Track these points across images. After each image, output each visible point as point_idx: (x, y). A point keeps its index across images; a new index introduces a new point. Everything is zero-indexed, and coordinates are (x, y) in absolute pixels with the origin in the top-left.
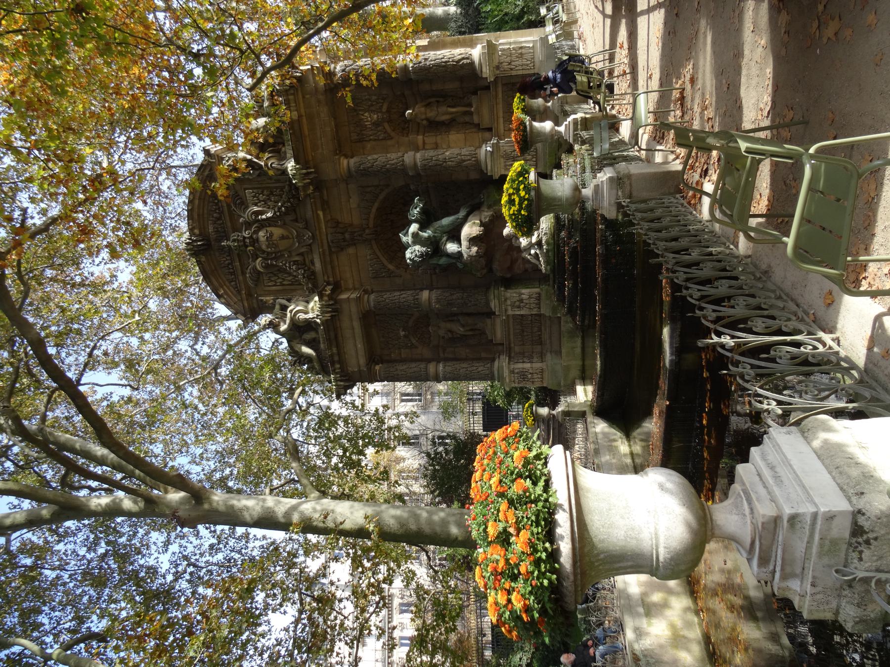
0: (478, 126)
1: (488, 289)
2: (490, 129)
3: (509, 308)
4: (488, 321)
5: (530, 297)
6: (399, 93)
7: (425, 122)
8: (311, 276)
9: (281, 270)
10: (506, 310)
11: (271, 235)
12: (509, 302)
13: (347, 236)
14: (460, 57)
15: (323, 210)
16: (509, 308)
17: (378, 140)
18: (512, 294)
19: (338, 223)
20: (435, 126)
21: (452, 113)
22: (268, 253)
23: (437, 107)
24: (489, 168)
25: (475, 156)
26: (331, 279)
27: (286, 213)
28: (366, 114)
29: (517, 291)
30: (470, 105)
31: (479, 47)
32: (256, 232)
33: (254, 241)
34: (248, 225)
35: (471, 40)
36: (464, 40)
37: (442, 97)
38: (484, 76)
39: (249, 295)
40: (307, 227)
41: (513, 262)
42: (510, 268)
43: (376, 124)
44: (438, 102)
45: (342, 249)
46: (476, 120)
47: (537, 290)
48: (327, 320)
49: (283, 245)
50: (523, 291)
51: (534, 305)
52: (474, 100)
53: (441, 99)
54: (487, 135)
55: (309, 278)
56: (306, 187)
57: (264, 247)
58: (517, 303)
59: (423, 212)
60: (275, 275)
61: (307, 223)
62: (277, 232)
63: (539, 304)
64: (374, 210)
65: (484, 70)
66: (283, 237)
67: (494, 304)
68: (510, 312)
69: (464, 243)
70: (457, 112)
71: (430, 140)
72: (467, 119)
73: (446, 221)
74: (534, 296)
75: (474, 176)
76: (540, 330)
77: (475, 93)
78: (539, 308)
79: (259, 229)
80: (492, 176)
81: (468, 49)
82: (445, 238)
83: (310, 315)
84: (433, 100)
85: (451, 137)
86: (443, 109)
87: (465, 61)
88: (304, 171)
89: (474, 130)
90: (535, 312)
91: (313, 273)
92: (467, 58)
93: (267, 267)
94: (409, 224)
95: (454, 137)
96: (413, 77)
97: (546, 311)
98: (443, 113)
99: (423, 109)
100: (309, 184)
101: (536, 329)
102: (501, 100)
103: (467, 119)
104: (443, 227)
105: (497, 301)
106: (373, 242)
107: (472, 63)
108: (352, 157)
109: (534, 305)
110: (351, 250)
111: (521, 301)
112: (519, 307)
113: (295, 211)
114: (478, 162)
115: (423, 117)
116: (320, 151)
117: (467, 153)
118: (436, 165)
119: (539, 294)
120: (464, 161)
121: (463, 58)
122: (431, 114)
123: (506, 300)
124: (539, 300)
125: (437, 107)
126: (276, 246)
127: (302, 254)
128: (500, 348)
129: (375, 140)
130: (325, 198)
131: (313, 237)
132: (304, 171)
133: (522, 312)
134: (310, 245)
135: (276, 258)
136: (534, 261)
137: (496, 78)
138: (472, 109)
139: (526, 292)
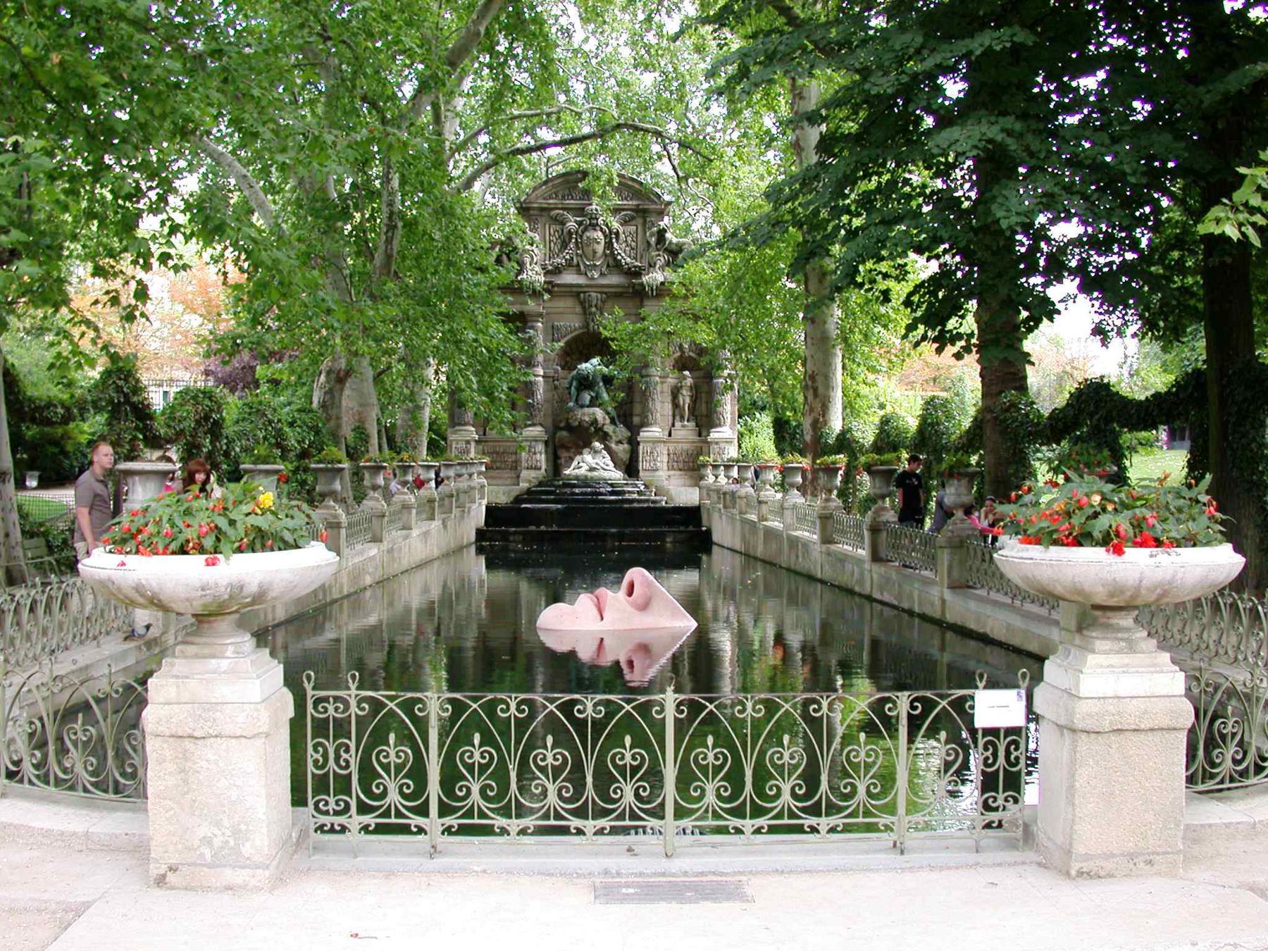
0: (673, 425)
2: (670, 435)
8: (557, 270)
9: (564, 245)
13: (594, 309)
18: (540, 447)
19: (603, 302)
20: (675, 393)
27: (615, 259)
33: (594, 226)
37: (695, 400)
39: (542, 209)
40: (602, 274)
41: (567, 449)
43: (681, 347)
45: (582, 303)
46: (678, 424)
47: (544, 467)
49: (589, 251)
50: (543, 456)
52: (692, 424)
55: (557, 268)
56: (642, 284)
57: (588, 234)
62: (600, 248)
66: (595, 252)
69: (592, 410)
71: (667, 389)
72: (678, 418)
73: (605, 396)
75: (636, 420)
76: (498, 468)
79: (604, 233)
86: (688, 400)
90: (524, 464)
91: (560, 272)
93: (570, 233)
95: (668, 407)
97: (525, 474)
98: (685, 399)
103: (678, 418)
107: (720, 425)
110: (578, 309)
126: (588, 246)
127: (578, 265)
131: (593, 278)
136: (575, 463)
139: (542, 459)
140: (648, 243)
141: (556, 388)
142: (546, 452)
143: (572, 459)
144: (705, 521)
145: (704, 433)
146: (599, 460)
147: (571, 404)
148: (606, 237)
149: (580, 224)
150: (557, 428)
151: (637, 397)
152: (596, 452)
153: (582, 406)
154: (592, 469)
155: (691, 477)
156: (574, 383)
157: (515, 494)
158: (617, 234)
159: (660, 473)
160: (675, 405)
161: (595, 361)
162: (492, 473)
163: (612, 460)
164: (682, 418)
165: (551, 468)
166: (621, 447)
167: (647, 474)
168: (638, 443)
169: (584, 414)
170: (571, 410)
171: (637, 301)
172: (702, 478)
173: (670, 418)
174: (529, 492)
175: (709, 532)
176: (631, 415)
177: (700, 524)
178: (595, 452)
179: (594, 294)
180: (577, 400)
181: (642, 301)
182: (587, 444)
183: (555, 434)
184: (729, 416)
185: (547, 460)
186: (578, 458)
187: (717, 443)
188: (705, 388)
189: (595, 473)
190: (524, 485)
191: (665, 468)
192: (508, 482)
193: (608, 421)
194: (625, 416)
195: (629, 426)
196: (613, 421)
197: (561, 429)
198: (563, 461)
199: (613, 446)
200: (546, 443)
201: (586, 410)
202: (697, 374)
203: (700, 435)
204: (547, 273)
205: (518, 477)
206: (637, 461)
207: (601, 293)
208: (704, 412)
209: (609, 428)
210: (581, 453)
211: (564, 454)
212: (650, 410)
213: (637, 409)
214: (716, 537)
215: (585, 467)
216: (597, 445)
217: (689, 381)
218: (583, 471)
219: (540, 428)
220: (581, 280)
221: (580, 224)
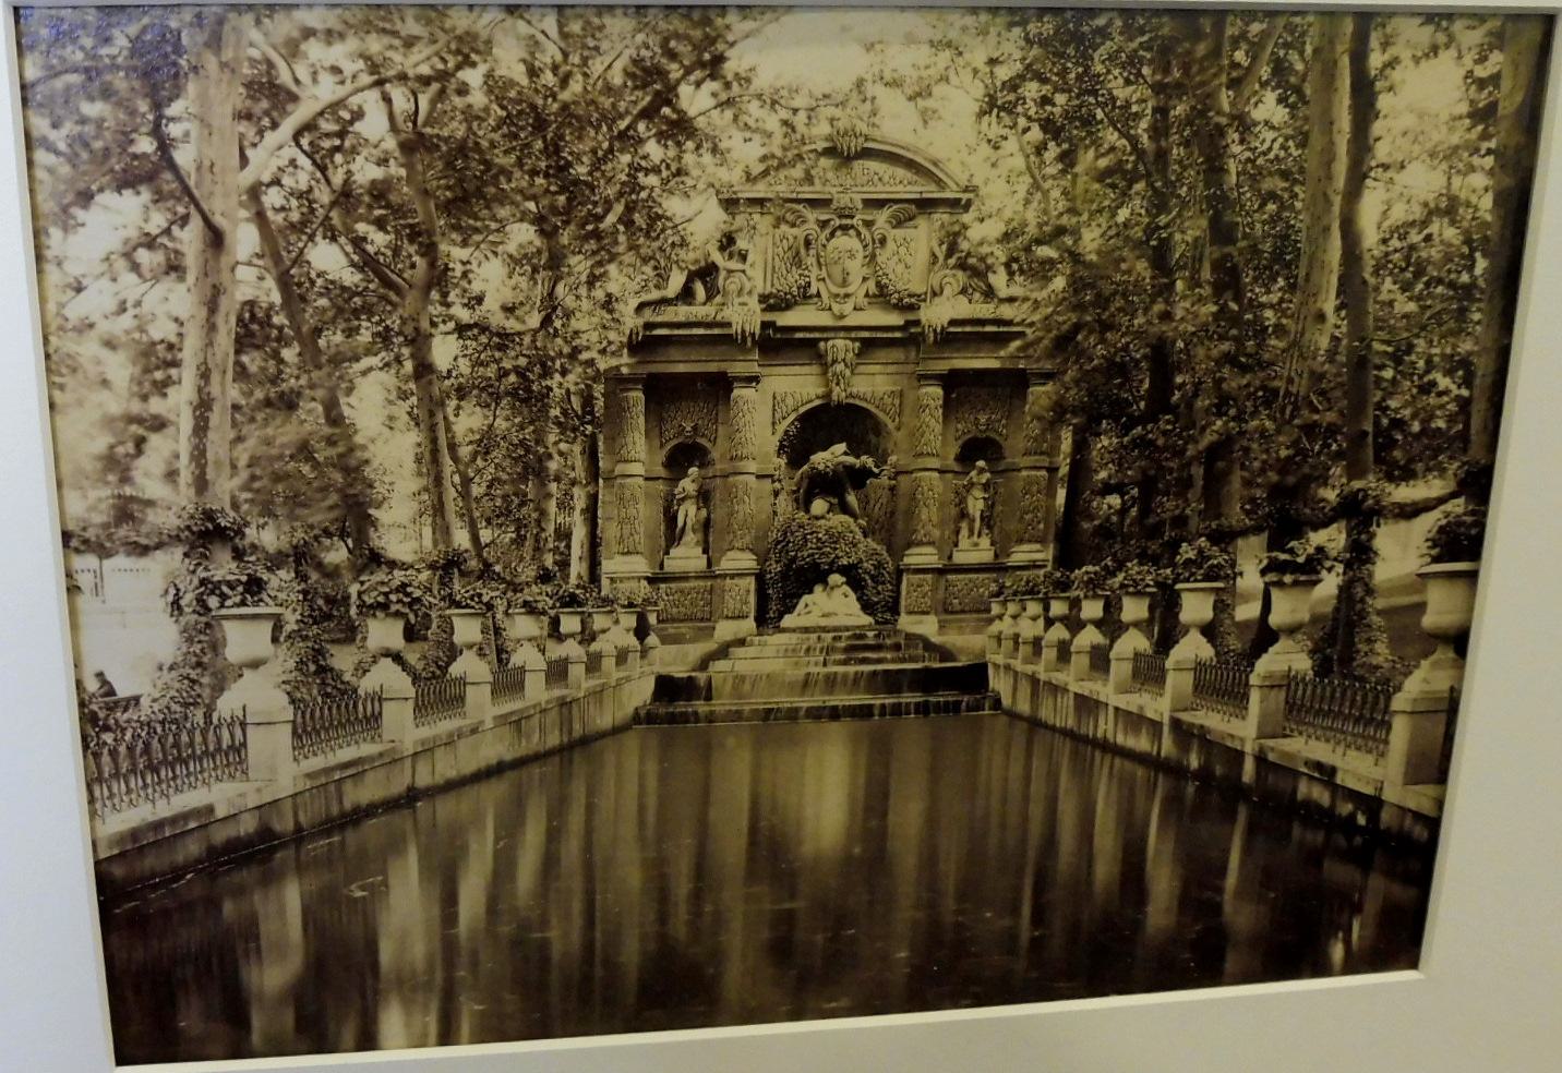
11: (852, 257)
22: (824, 246)
23: (984, 498)
32: (859, 234)
34: (869, 224)
59: (871, 474)
60: (790, 248)
62: (856, 268)
64: (869, 407)
70: (974, 521)
72: (964, 532)
77: (992, 545)
86: (980, 505)
94: (858, 457)
99: (984, 481)
100: (922, 333)
113: (881, 295)
127: (818, 295)
132: (939, 330)
134: (830, 309)
135: (818, 257)
140: (934, 255)
148: (865, 246)
149: (823, 224)
158: (883, 241)
161: (842, 447)
179: (840, 343)
186: (806, 598)
207: (853, 340)
215: (816, 612)
220: (824, 319)
221: (823, 224)
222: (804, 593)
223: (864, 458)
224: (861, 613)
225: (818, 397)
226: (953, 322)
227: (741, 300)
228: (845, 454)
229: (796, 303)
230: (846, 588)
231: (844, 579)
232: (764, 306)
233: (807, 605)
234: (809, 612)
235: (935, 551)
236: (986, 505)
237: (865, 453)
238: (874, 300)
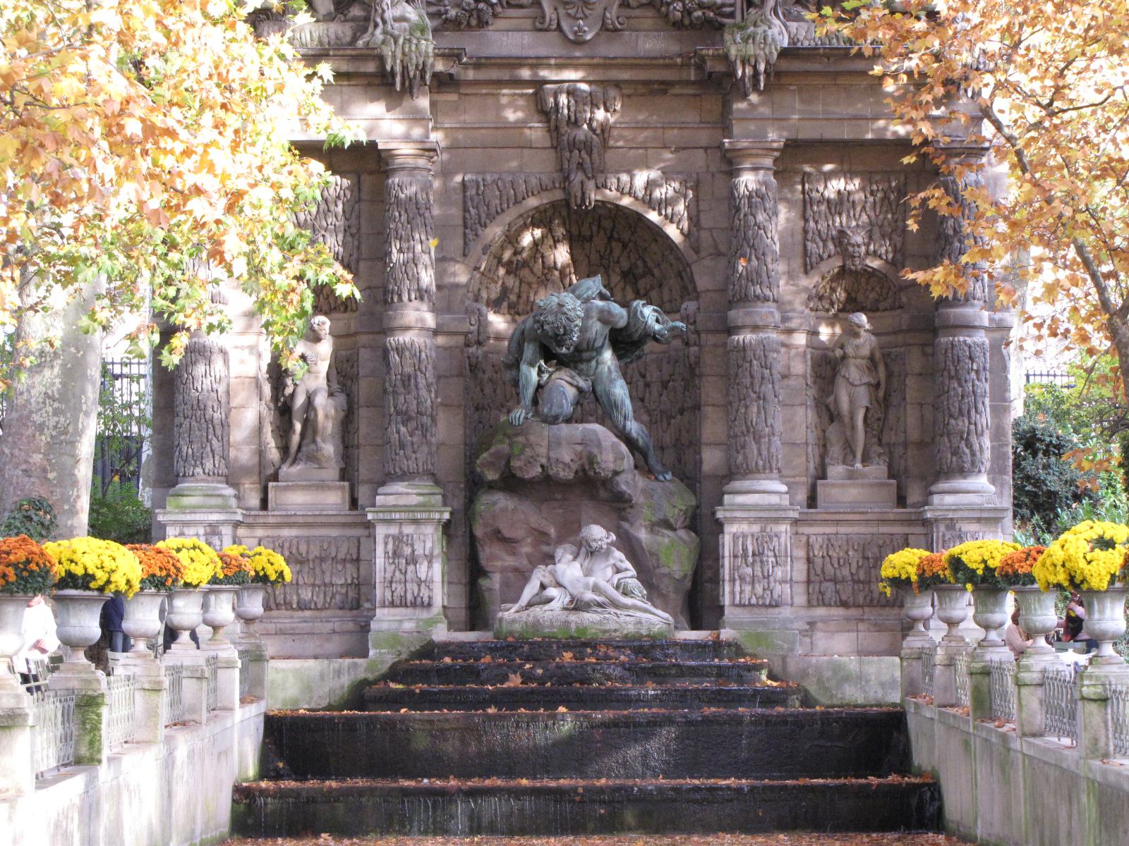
0: (822, 474)
1: (433, 475)
2: (812, 501)
3: (394, 530)
4: (331, 472)
5: (419, 582)
6: (904, 299)
7: (838, 353)
10: (389, 522)
12: (408, 529)
14: (976, 447)
15: (646, 83)
16: (394, 530)
17: (805, 239)
18: (428, 539)
21: (852, 418)
23: (869, 384)
24: (740, 499)
25: (767, 468)
26: (471, 74)
28: (864, 218)
29: (437, 551)
30: (866, 460)
31: (992, 488)
35: (1002, 471)
36: (1005, 455)
38: (936, 499)
42: (498, 536)
43: (841, 238)
44: (878, 385)
46: (836, 470)
47: (439, 599)
48: (381, 59)
50: (437, 568)
51: (399, 589)
52: (877, 470)
53: (881, 394)
54: (802, 496)
56: (726, 57)
58: (407, 551)
61: (616, 30)
63: (403, 604)
65: (949, 499)
67: (400, 494)
68: (381, 531)
70: (853, 427)
72: (835, 450)
73: (620, 390)
74: (425, 593)
75: (711, 459)
76: (302, 606)
77: (891, 476)
78: (392, 604)
80: (721, 503)
81: (988, 465)
82: (582, 383)
83: (389, 14)
84: (882, 369)
85: (801, 411)
87: (968, 458)
88: (762, 67)
89: (812, 466)
91: (482, 24)
92: (973, 463)
94: (625, 305)
96: (944, 340)
97: (385, 620)
99: (866, 352)
101: (306, 594)
102: (874, 530)
103: (835, 450)
104: (612, 381)
105: (415, 500)
106: (558, 195)
107: (962, 472)
108: (776, 174)
109: (399, 589)
111: (413, 560)
112: (396, 554)
114: (748, 472)
115: (850, 351)
116: (798, 105)
117: (773, 450)
118: (752, 377)
119: (430, 605)
120: (758, 442)
121: (973, 454)
122: (854, 372)
123: (415, 522)
124: (414, 605)
125: (869, 384)
128: (254, 501)
129: (805, 231)
130: (677, 90)
131: (579, 43)
132: (762, 67)
133: (380, 561)
134: (559, 28)
137: (926, 523)
138: (859, 465)
141: (474, 368)
142: (448, 559)
143: (523, 576)
144: (921, 756)
145: (914, 496)
146: (604, 575)
147: (519, 414)
150: (474, 485)
151: (710, 390)
152: (592, 553)
153: (553, 420)
154: (578, 605)
155: (879, 628)
156: (529, 350)
157: (346, 681)
159: (786, 612)
160: (829, 413)
162: (284, 619)
163: (645, 575)
164: (849, 447)
165: (460, 602)
166: (666, 537)
167: (744, 615)
168: (719, 526)
169: (555, 443)
170: (521, 430)
171: (712, 104)
172: (908, 626)
173: (813, 451)
174: (394, 673)
175: (934, 789)
176: (695, 445)
177: (903, 762)
178: (591, 552)
180: (535, 402)
181: (726, 107)
182: (570, 532)
183: (470, 501)
184: (987, 442)
185: (448, 581)
186: (540, 575)
187: (951, 524)
188: (915, 362)
189: (588, 617)
190: (380, 657)
191: (801, 599)
192: (334, 645)
193: (629, 461)
194: (677, 444)
195: (689, 477)
196: (644, 465)
197: (492, 486)
198: (494, 583)
199: (643, 535)
200: (447, 528)
201: (565, 429)
202: (889, 320)
203: (901, 501)
204: (445, 25)
205: (364, 629)
206: (716, 580)
208: (914, 435)
209: (632, 483)
210: (549, 559)
211: (496, 560)
212: (750, 430)
213: (712, 427)
214: (955, 802)
215: (559, 598)
216: (597, 533)
217: (866, 342)
218: (554, 612)
219: (426, 486)
222: (534, 564)
223: (638, 304)
224: (649, 606)
225: (543, 189)
226: (784, 53)
227: (397, 12)
228: (602, 297)
229: (495, 16)
230: (619, 555)
231: (613, 537)
232: (436, 22)
233: (543, 587)
234: (550, 600)
235: (784, 488)
236: (874, 399)
237: (638, 296)
238: (638, 12)
